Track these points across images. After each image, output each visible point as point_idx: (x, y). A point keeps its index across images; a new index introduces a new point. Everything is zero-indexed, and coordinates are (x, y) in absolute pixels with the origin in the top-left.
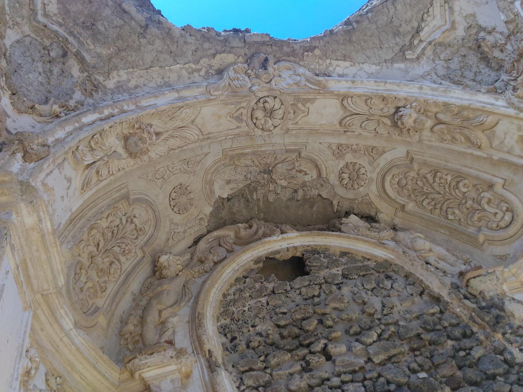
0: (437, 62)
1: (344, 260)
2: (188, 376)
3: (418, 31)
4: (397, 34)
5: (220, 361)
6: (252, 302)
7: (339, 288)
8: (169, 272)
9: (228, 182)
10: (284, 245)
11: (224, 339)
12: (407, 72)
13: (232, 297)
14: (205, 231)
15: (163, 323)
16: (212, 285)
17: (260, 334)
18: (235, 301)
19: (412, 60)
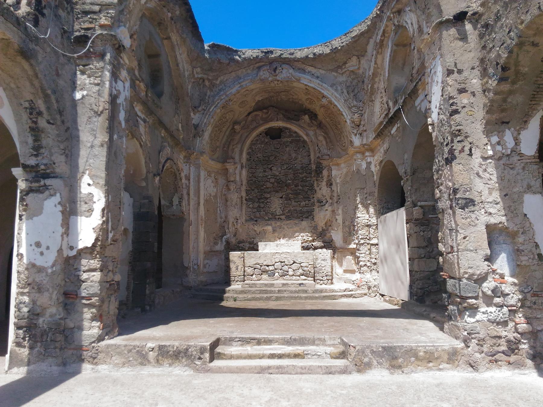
0: (349, 78)
1: (294, 135)
2: (236, 168)
3: (345, 63)
4: (336, 61)
5: (244, 165)
6: (259, 145)
7: (286, 147)
8: (237, 131)
9: (262, 96)
10: (276, 125)
11: (248, 157)
12: (336, 77)
13: (254, 142)
14: (252, 110)
15: (234, 149)
16: (248, 140)
17: (258, 157)
18: (254, 144)
19: (340, 73)
